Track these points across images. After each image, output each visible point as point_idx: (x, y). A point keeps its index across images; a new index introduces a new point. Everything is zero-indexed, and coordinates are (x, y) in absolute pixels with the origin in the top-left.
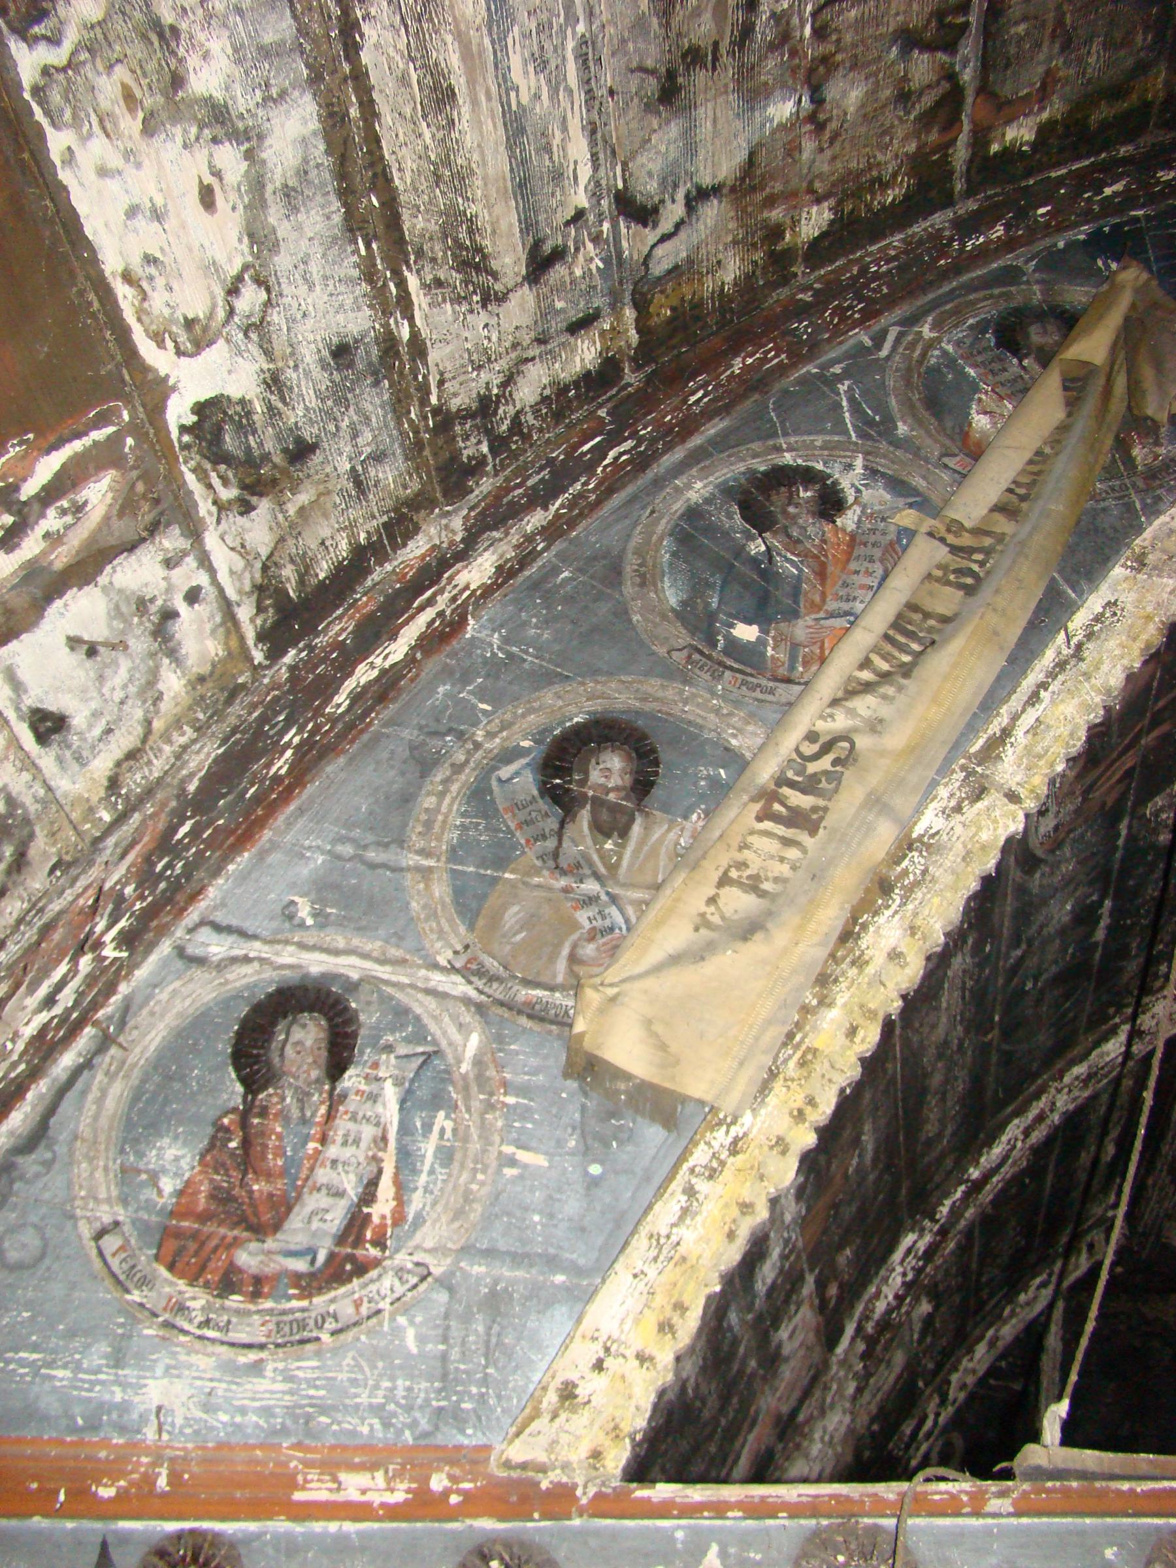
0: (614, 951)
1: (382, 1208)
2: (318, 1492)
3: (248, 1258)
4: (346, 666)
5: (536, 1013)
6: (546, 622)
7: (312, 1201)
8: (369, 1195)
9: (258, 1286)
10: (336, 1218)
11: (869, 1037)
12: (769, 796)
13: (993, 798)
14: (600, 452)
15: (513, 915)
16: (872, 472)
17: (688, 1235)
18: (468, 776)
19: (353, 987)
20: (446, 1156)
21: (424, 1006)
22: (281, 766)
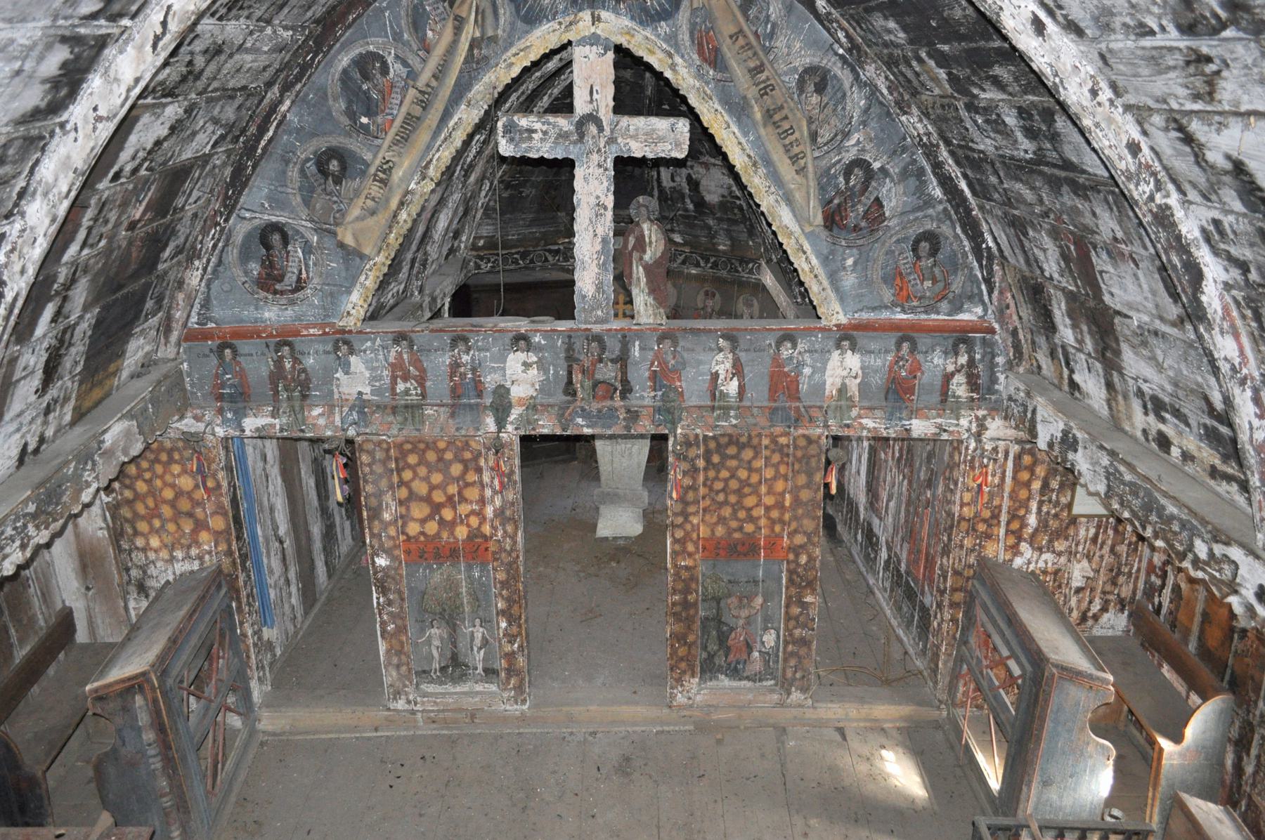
0: (343, 215)
1: (304, 276)
2: (305, 333)
3: (278, 287)
4: (258, 141)
5: (329, 231)
6: (309, 114)
7: (289, 275)
8: (300, 273)
9: (282, 293)
10: (295, 278)
11: (400, 240)
12: (375, 175)
13: (427, 180)
14: (313, 59)
15: (318, 206)
16: (397, 57)
17: (367, 283)
18: (298, 166)
19: (283, 225)
20: (315, 264)
21: (302, 230)
22: (249, 171)
